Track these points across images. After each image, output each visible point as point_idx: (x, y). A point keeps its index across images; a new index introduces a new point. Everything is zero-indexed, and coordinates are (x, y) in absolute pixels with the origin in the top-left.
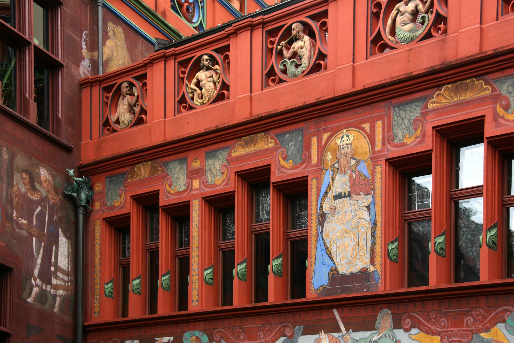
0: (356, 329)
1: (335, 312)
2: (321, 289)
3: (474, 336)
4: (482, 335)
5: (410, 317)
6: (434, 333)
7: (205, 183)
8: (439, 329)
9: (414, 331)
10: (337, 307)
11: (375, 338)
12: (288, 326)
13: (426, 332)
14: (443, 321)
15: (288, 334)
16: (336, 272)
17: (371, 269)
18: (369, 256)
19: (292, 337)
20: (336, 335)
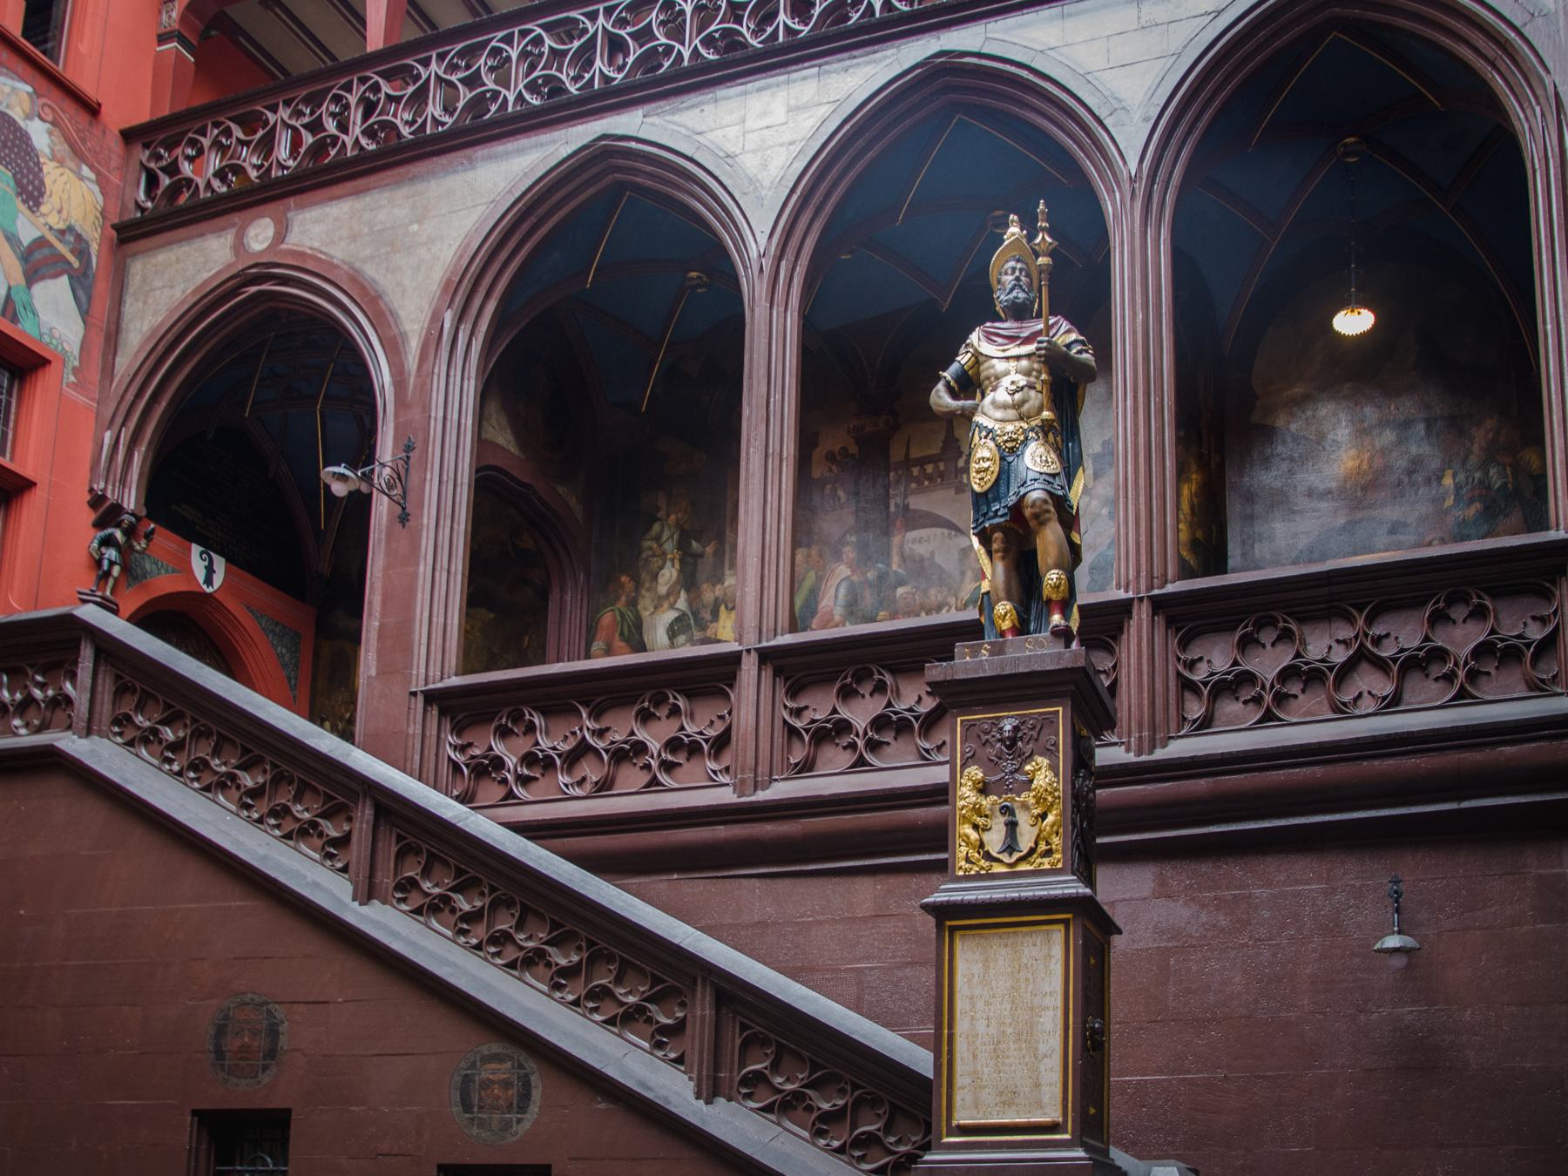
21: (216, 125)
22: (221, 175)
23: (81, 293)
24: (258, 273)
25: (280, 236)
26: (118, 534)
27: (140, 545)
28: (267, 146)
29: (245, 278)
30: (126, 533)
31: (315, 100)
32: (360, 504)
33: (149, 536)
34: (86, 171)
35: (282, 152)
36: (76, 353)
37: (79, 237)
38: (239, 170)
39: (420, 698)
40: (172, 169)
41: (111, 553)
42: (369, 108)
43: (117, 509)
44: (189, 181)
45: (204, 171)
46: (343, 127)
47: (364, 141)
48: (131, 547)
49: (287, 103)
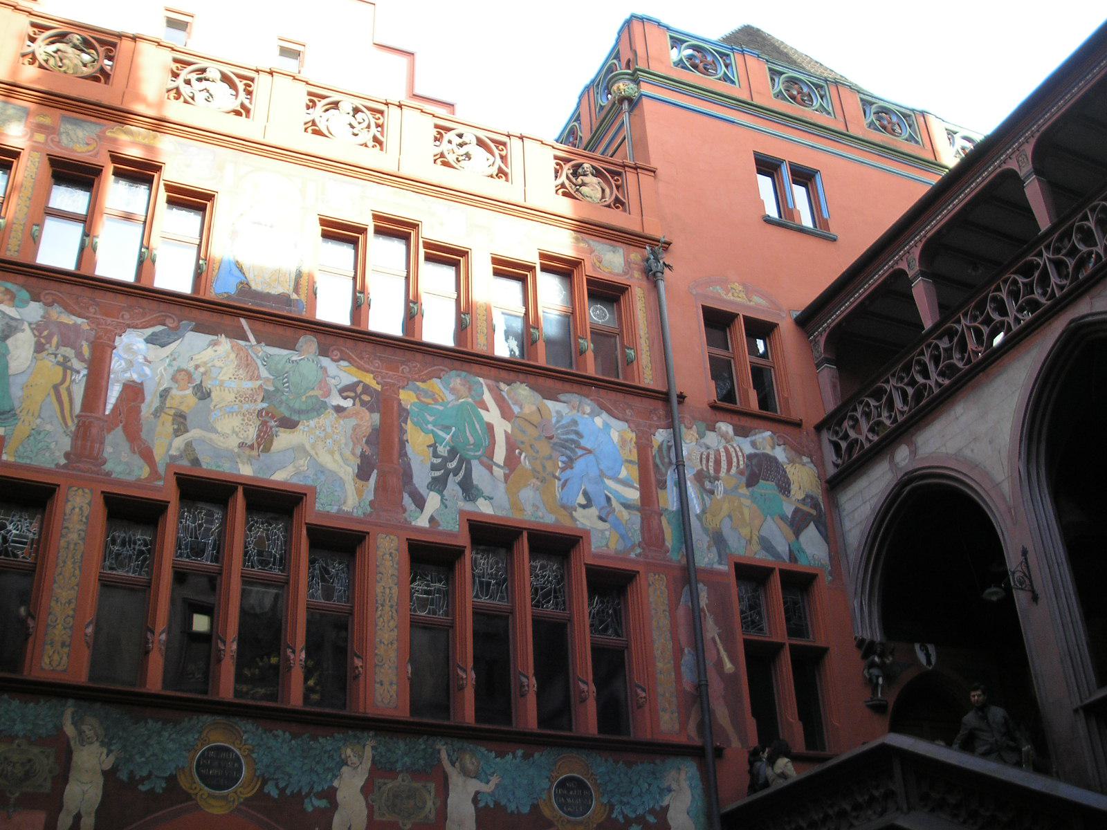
0: (270, 344)
1: (243, 321)
2: (226, 295)
3: (410, 383)
4: (418, 384)
5: (341, 351)
6: (367, 371)
7: (58, 143)
8: (372, 368)
9: (343, 363)
10: (246, 317)
11: (294, 358)
12: (170, 317)
13: (359, 368)
14: (377, 363)
15: (171, 325)
16: (246, 286)
17: (294, 296)
18: (292, 284)
19: (177, 328)
20: (242, 343)
21: (861, 402)
22: (871, 430)
23: (820, 527)
24: (909, 479)
25: (914, 453)
26: (876, 659)
27: (889, 660)
28: (890, 404)
29: (902, 484)
30: (880, 656)
31: (907, 368)
32: (1009, 600)
33: (892, 653)
34: (805, 459)
35: (898, 404)
36: (828, 562)
37: (812, 498)
38: (879, 423)
39: (1081, 712)
40: (846, 436)
41: (875, 671)
42: (936, 359)
43: (872, 643)
44: (856, 440)
45: (864, 434)
46: (927, 376)
47: (940, 380)
48: (885, 663)
49: (893, 375)
